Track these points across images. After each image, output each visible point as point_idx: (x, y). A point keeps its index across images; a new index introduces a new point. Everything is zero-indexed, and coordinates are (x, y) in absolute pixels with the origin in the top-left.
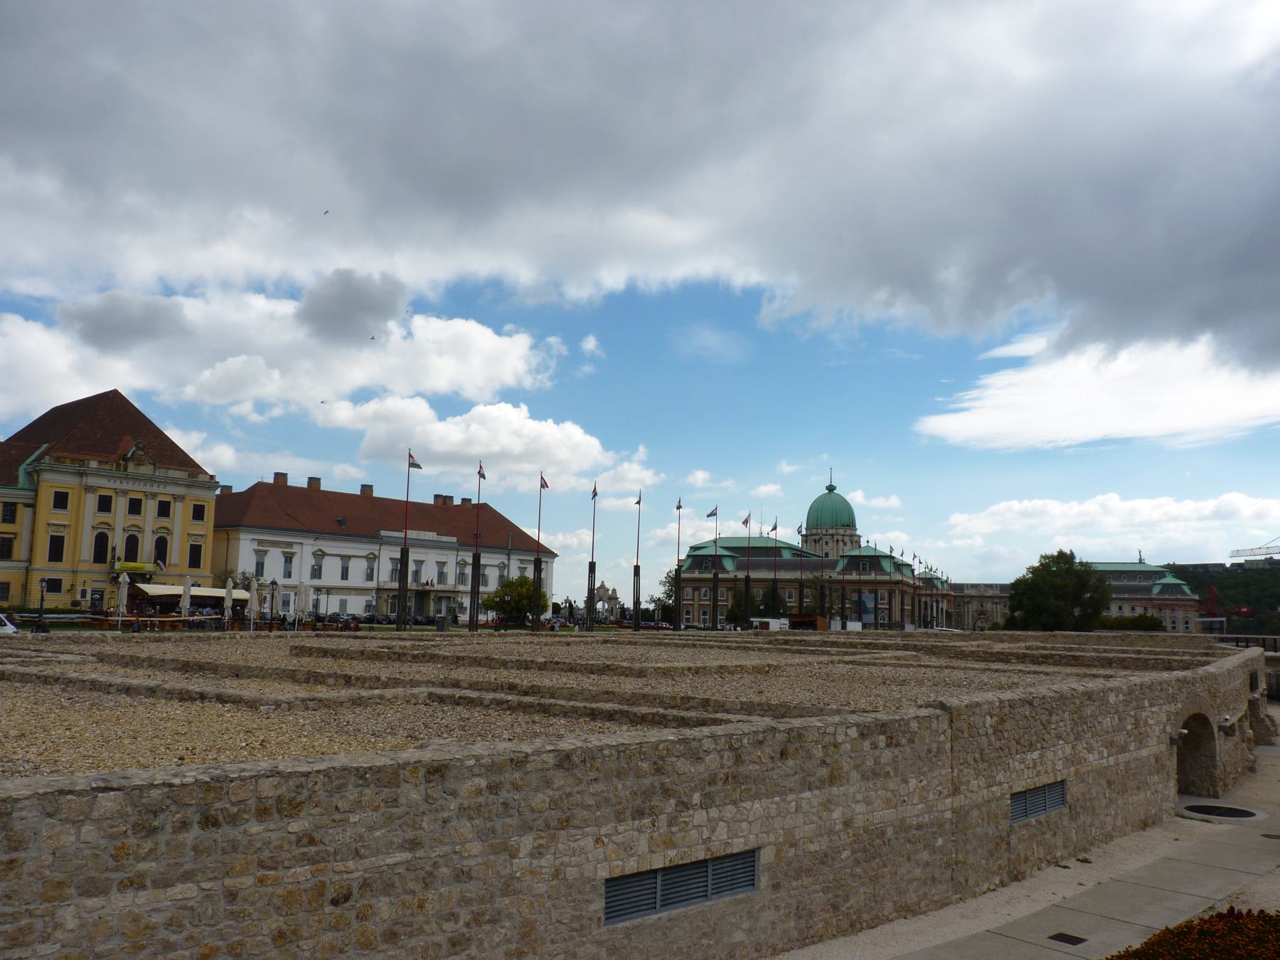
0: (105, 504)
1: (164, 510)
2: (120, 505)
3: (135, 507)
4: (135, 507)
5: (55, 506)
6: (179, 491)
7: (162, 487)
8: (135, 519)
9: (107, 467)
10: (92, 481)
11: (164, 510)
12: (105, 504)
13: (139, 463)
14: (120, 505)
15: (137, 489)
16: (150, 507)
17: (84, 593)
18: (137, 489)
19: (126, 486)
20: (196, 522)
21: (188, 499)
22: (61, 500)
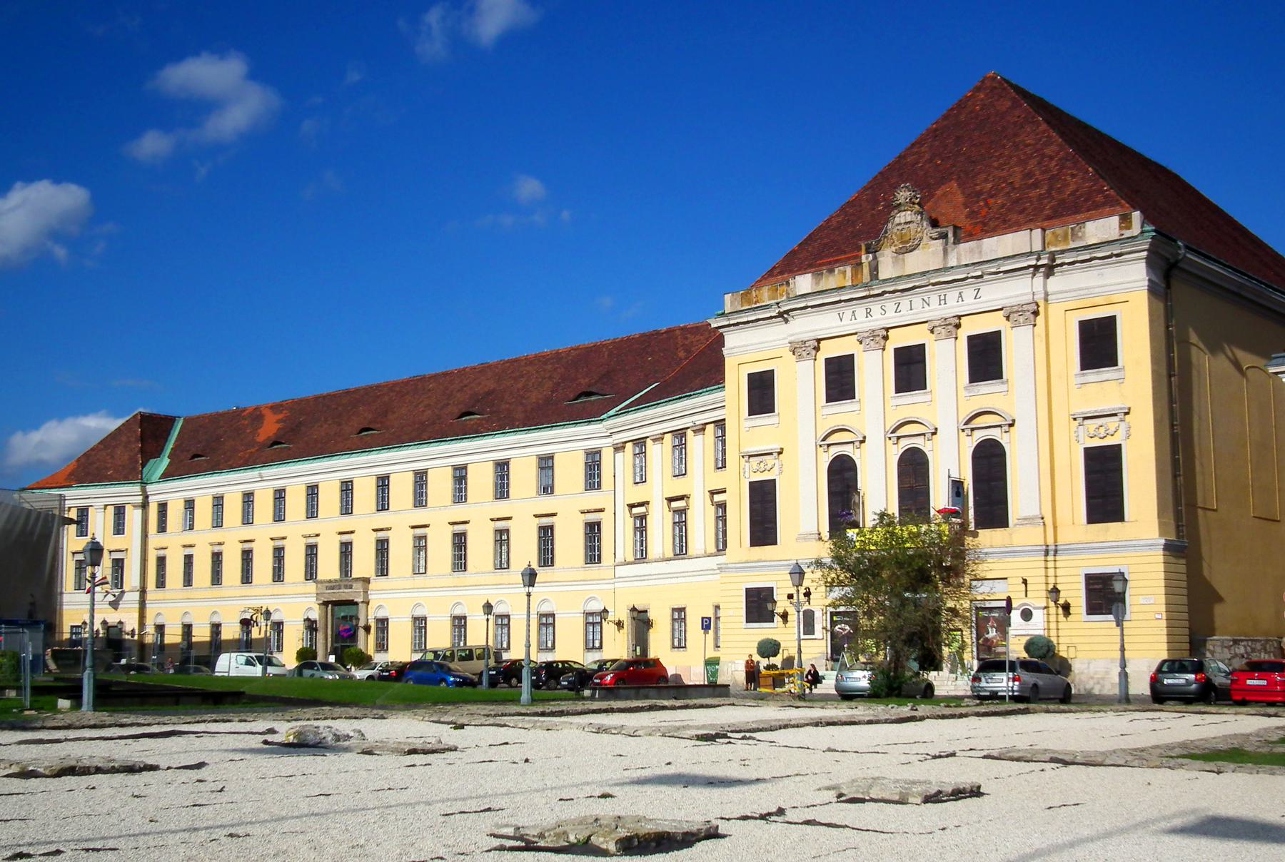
0: (840, 379)
1: (985, 359)
2: (874, 372)
3: (910, 370)
4: (910, 370)
5: (753, 411)
6: (1021, 289)
7: (969, 293)
8: (911, 404)
9: (831, 281)
10: (805, 326)
11: (985, 359)
12: (840, 379)
13: (908, 247)
14: (874, 372)
15: (907, 317)
16: (947, 362)
17: (809, 620)
18: (907, 317)
19: (882, 314)
20: (1092, 375)
21: (1055, 311)
22: (762, 393)
